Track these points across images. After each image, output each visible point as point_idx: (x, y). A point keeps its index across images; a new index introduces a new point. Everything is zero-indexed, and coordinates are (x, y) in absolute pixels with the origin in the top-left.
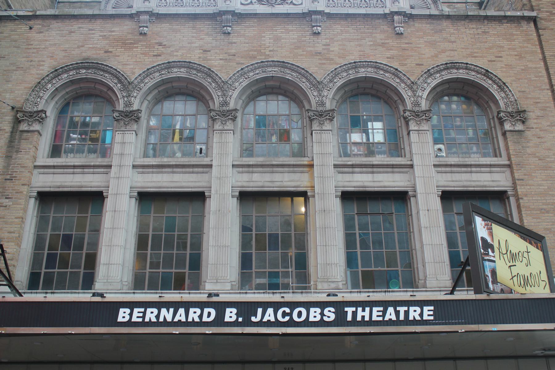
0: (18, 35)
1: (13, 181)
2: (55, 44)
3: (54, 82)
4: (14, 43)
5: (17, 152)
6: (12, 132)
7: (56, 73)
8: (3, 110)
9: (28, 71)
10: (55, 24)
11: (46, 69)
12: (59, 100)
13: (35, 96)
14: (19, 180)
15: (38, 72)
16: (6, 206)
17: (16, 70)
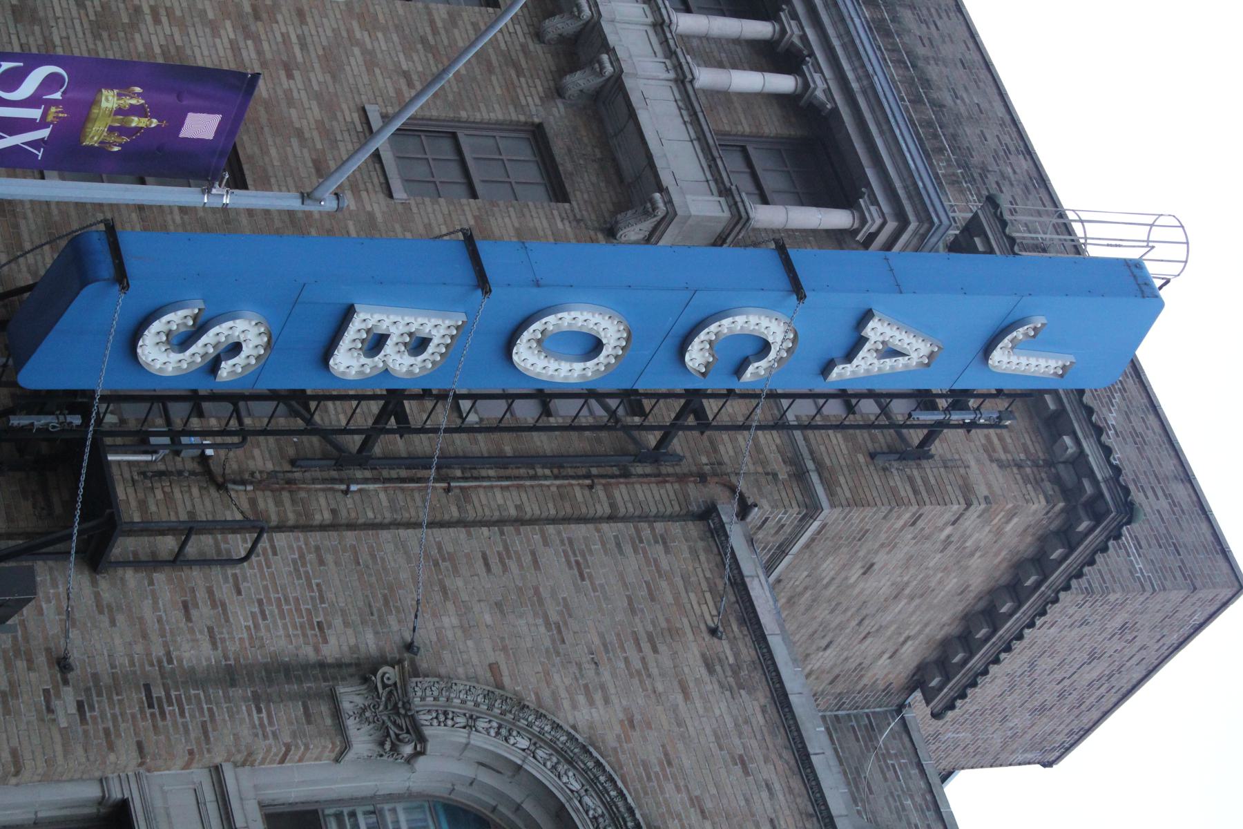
0: (677, 597)
1: (148, 711)
2: (680, 723)
3: (540, 753)
4: (644, 592)
5: (256, 698)
6: (322, 665)
7: (576, 752)
8: (392, 620)
9: (557, 660)
10: (755, 704)
11: (582, 715)
12: (485, 787)
13: (470, 704)
14: (155, 727)
15: (563, 694)
16: (50, 710)
17: (548, 624)
